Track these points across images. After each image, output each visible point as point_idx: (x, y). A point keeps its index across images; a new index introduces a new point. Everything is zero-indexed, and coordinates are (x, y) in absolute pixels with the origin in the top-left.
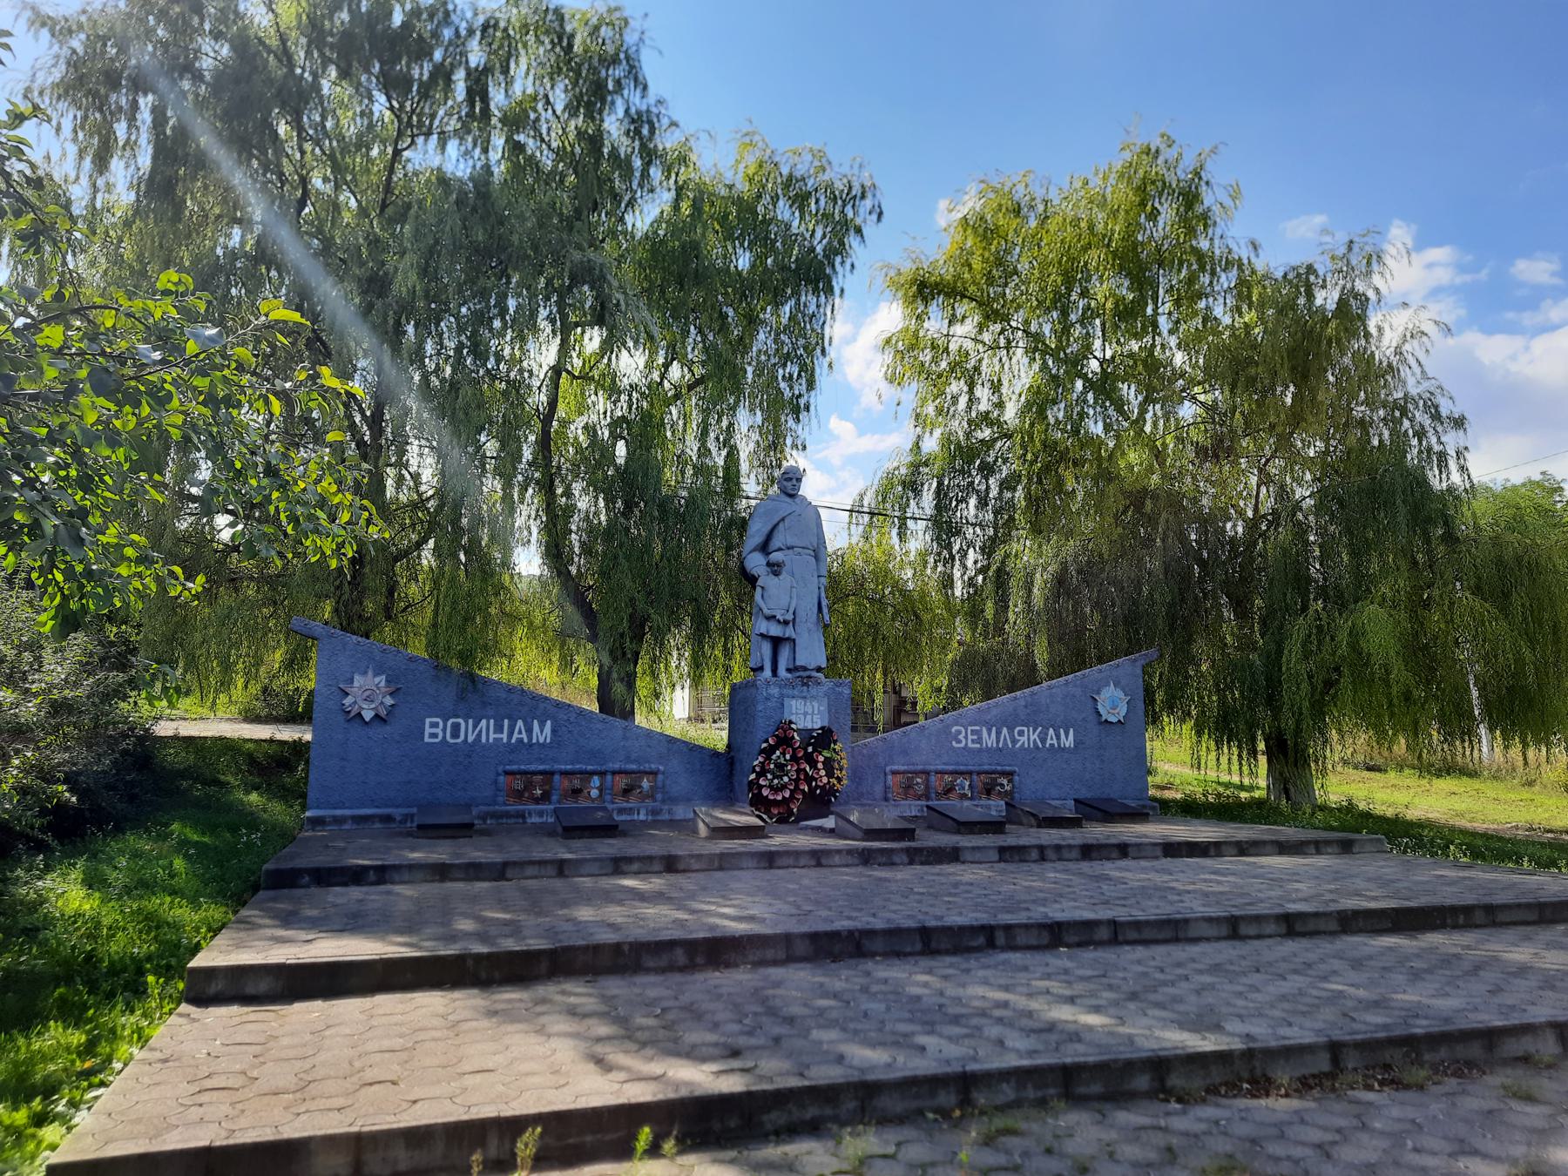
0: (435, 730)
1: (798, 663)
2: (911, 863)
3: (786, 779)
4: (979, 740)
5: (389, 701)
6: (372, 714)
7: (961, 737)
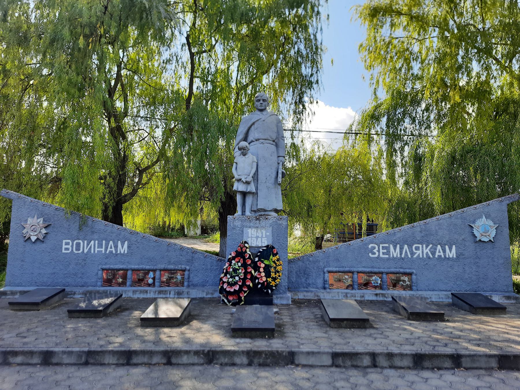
0: (67, 246)
1: (259, 207)
2: (250, 364)
3: (237, 278)
4: (388, 253)
5: (44, 231)
6: (35, 238)
7: (375, 251)
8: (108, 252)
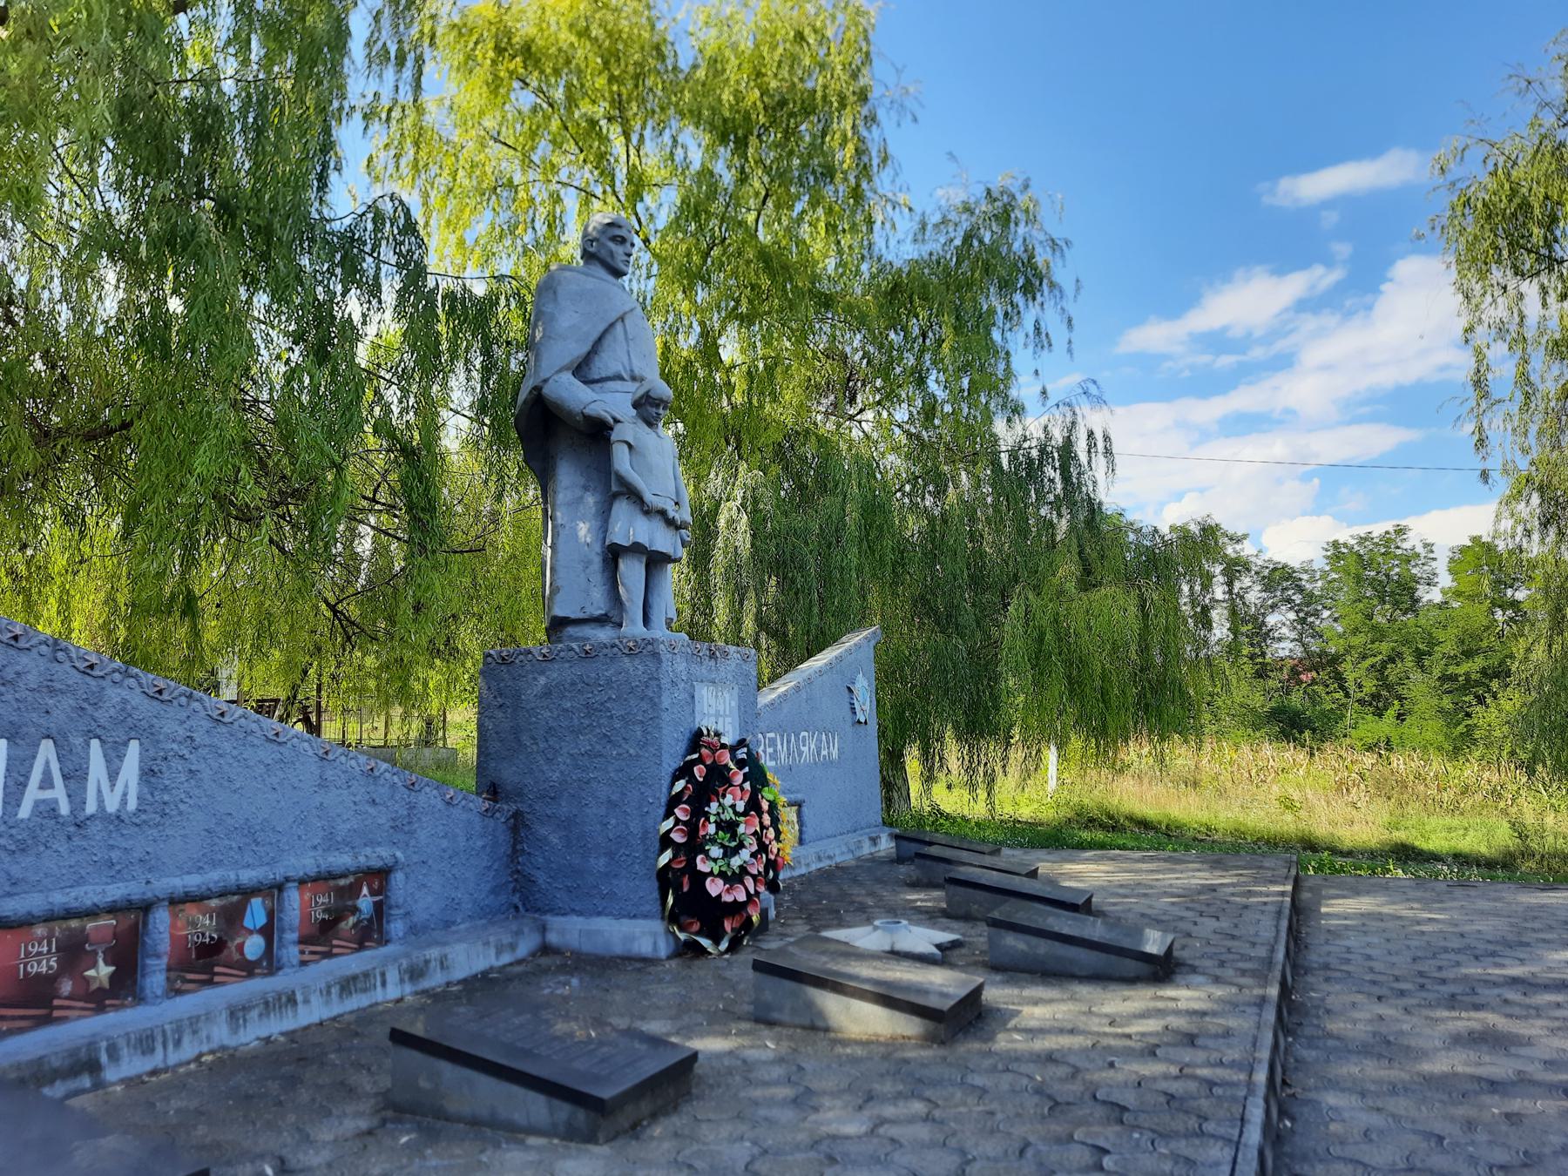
8: (24, 812)
